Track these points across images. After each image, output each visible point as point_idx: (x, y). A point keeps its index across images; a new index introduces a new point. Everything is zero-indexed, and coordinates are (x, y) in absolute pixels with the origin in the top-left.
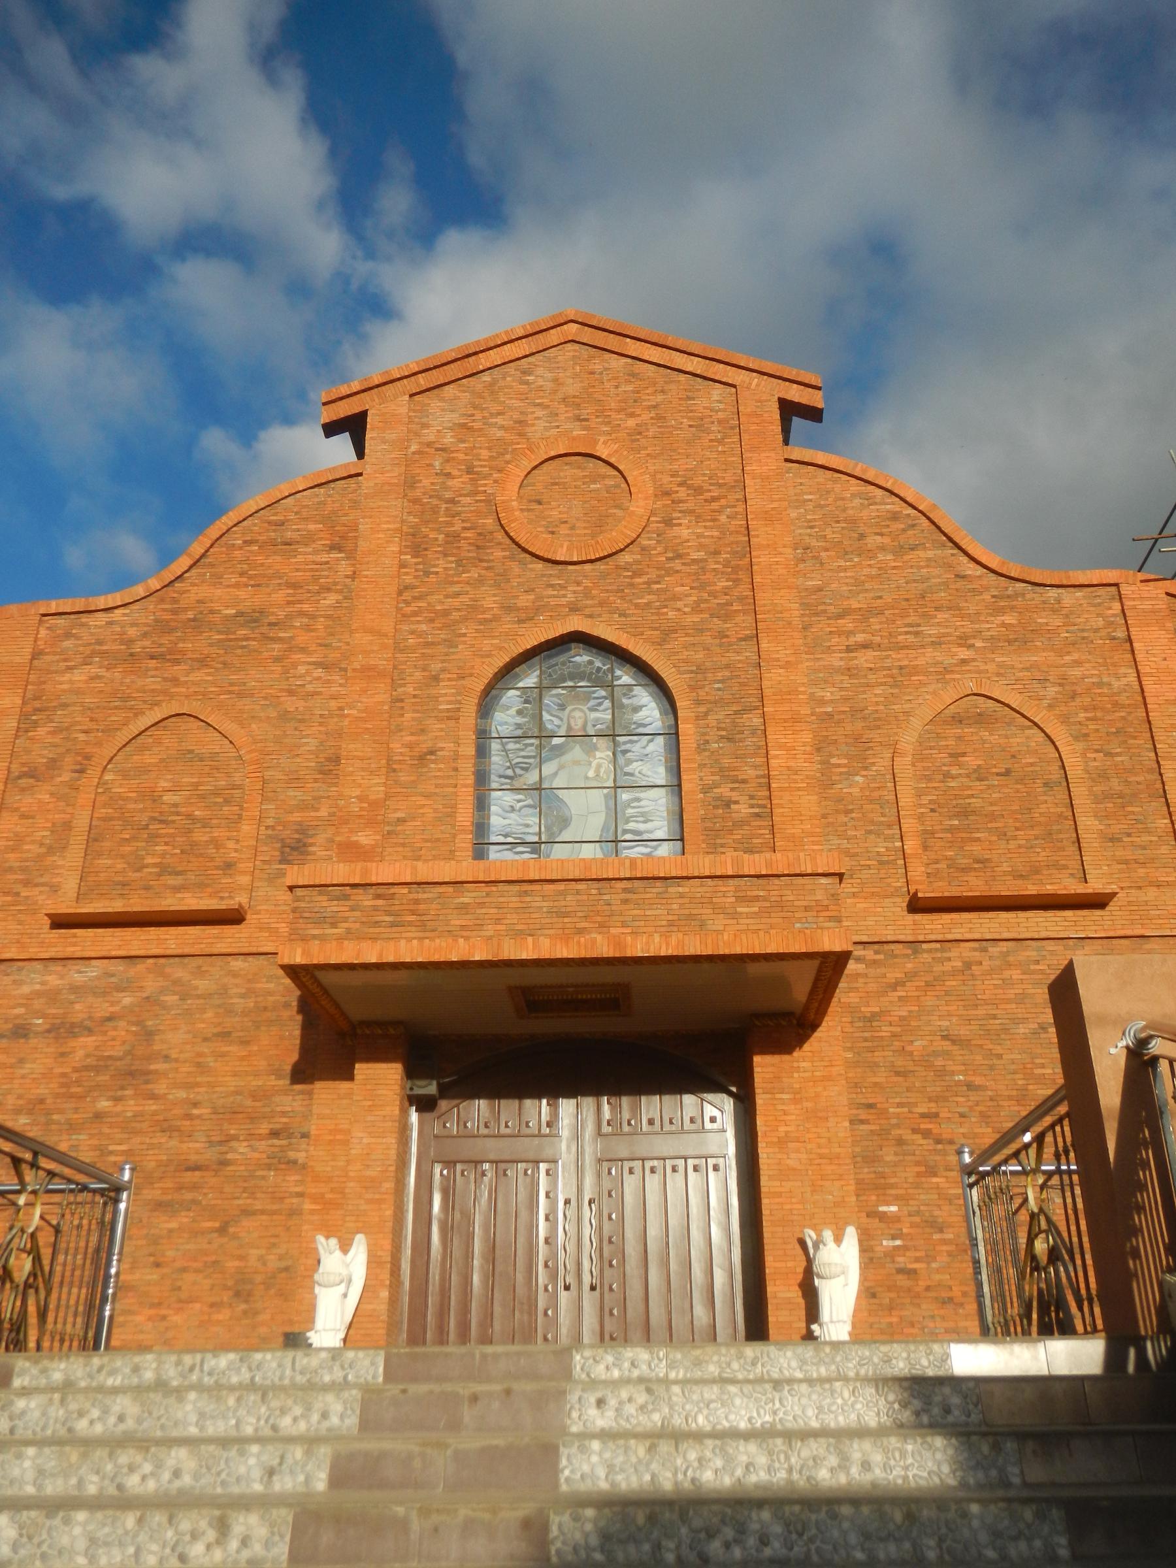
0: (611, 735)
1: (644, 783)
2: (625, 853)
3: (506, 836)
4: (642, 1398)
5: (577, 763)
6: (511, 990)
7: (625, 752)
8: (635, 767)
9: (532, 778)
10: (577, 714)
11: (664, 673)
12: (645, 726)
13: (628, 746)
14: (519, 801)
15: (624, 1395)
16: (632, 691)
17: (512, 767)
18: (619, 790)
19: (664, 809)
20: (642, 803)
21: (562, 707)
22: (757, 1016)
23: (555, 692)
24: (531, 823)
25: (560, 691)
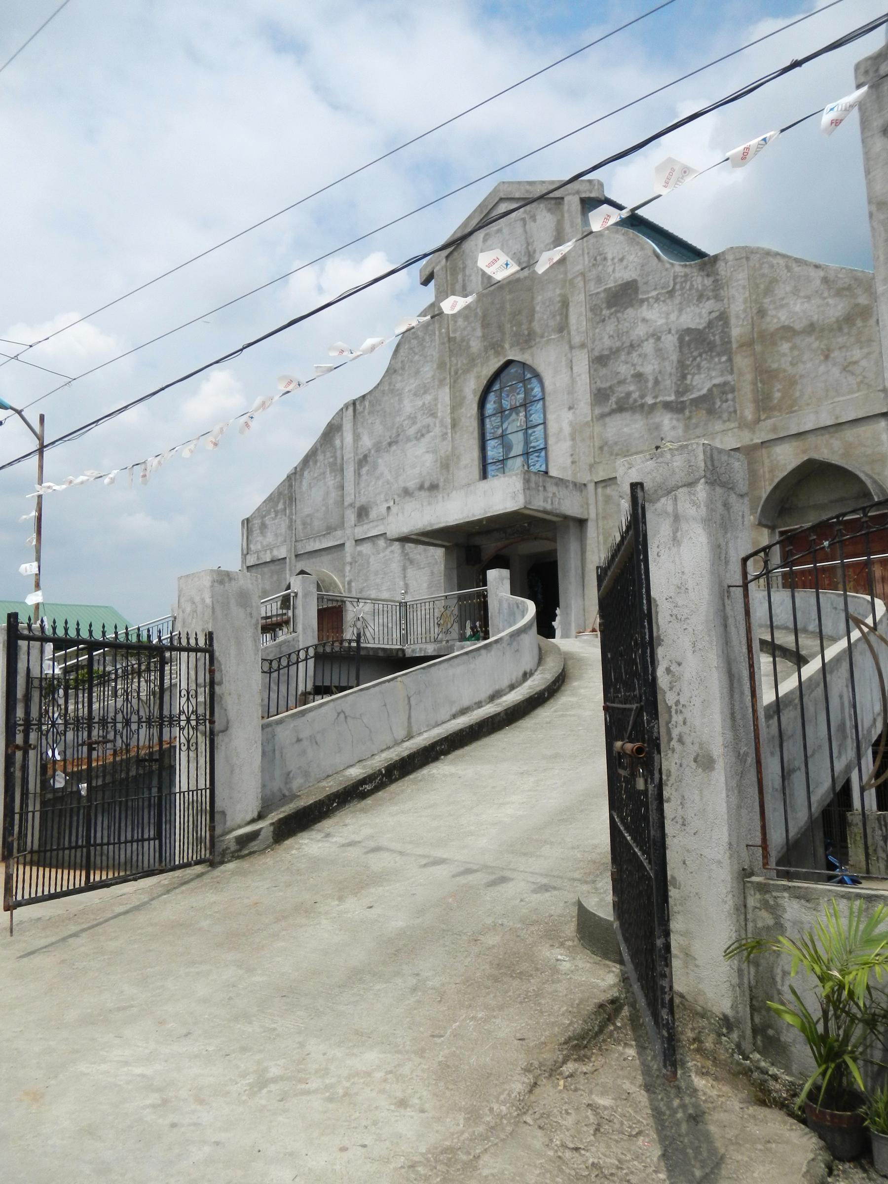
2: (531, 457)
5: (514, 420)
9: (500, 431)
21: (508, 396)
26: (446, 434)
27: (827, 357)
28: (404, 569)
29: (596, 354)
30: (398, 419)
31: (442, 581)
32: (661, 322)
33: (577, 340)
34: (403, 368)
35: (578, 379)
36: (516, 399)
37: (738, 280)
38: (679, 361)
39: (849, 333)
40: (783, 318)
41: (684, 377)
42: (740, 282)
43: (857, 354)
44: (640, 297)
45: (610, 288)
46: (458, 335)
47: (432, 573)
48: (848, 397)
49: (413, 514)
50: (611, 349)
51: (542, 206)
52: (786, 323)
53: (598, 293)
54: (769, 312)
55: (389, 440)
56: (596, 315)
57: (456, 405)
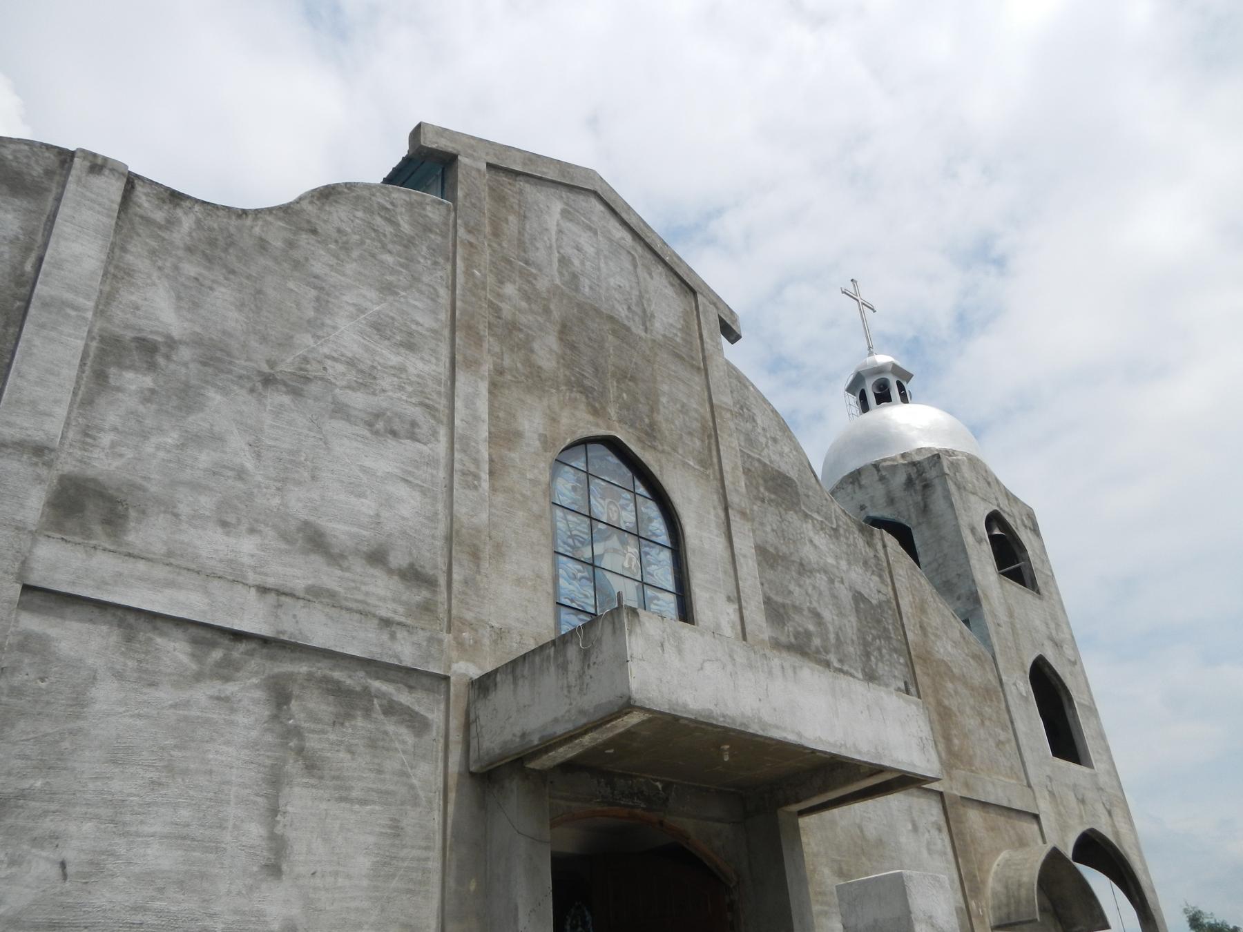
1: (659, 586)
3: (572, 601)
5: (615, 551)
7: (647, 554)
8: (652, 568)
9: (586, 554)
10: (614, 508)
12: (657, 536)
13: (647, 549)
14: (579, 571)
16: (647, 503)
17: (572, 537)
18: (645, 586)
20: (659, 603)
23: (597, 481)
24: (587, 593)
25: (600, 481)
26: (477, 477)
27: (983, 722)
28: (276, 780)
29: (759, 542)
30: (308, 340)
31: (435, 864)
32: (831, 561)
33: (733, 498)
34: (346, 247)
35: (742, 560)
36: (619, 516)
37: (900, 576)
38: (859, 630)
39: (990, 707)
40: (942, 650)
41: (868, 655)
42: (904, 580)
43: (1003, 736)
44: (803, 508)
45: (765, 465)
46: (506, 309)
47: (396, 830)
48: (1007, 780)
49: (707, 665)
50: (776, 548)
51: (660, 268)
52: (945, 659)
53: (753, 458)
54: (930, 635)
55: (265, 368)
56: (751, 483)
57: (505, 436)
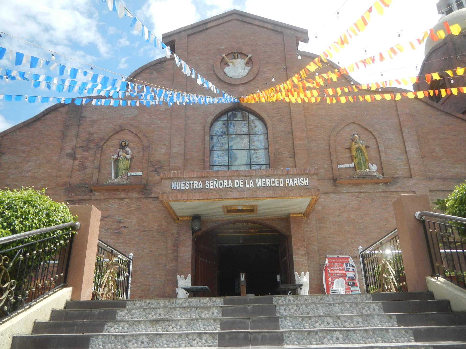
0: (249, 134)
1: (258, 148)
2: (253, 168)
3: (219, 163)
4: (295, 308)
6: (223, 207)
9: (226, 147)
10: (238, 128)
11: (263, 116)
12: (258, 132)
13: (253, 137)
15: (291, 307)
18: (251, 150)
19: (264, 155)
20: (257, 154)
22: (292, 214)
